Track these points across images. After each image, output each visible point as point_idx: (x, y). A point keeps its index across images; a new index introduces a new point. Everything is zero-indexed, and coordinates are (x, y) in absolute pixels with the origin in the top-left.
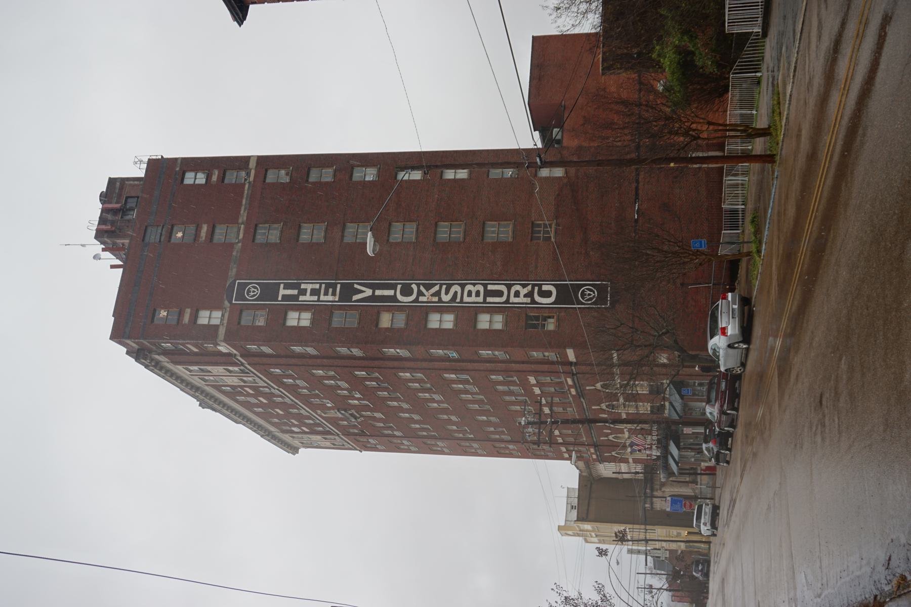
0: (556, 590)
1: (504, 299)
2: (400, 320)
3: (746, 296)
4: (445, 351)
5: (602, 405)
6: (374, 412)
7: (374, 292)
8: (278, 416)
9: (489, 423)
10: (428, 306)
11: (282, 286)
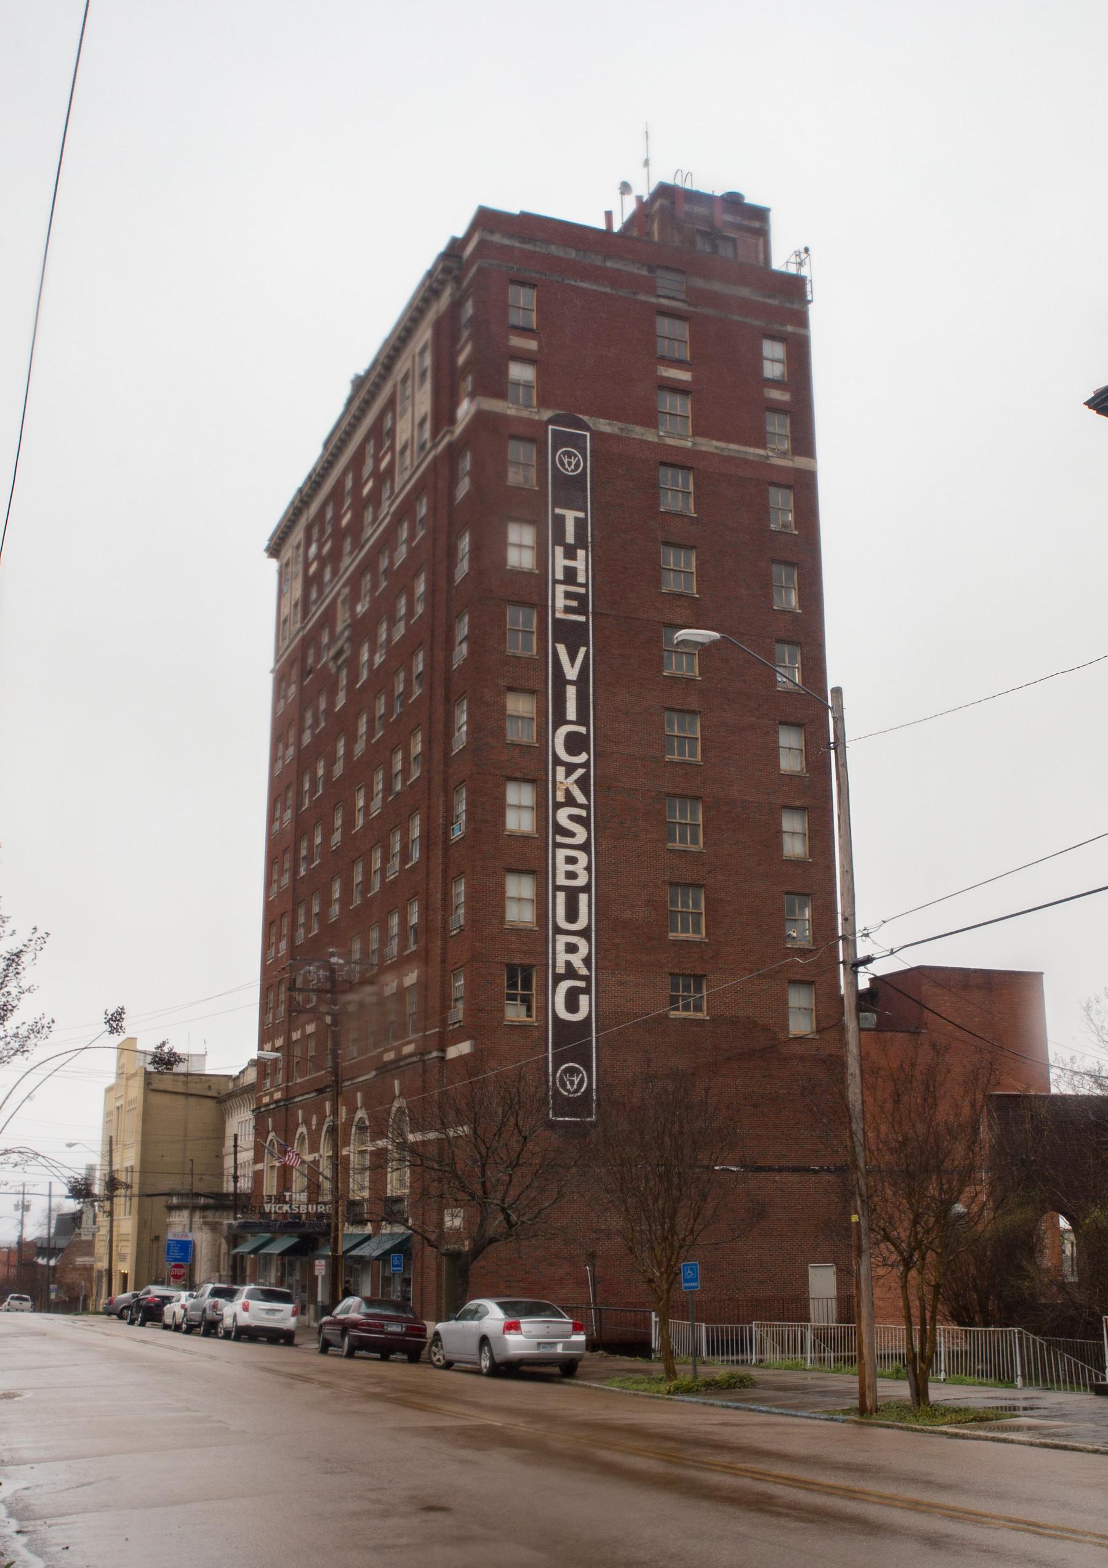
0: (34, 937)
1: (563, 924)
2: (520, 734)
3: (579, 1370)
4: (464, 817)
5: (364, 1111)
6: (347, 691)
7: (571, 683)
8: (337, 517)
9: (326, 903)
10: (548, 784)
11: (581, 515)
